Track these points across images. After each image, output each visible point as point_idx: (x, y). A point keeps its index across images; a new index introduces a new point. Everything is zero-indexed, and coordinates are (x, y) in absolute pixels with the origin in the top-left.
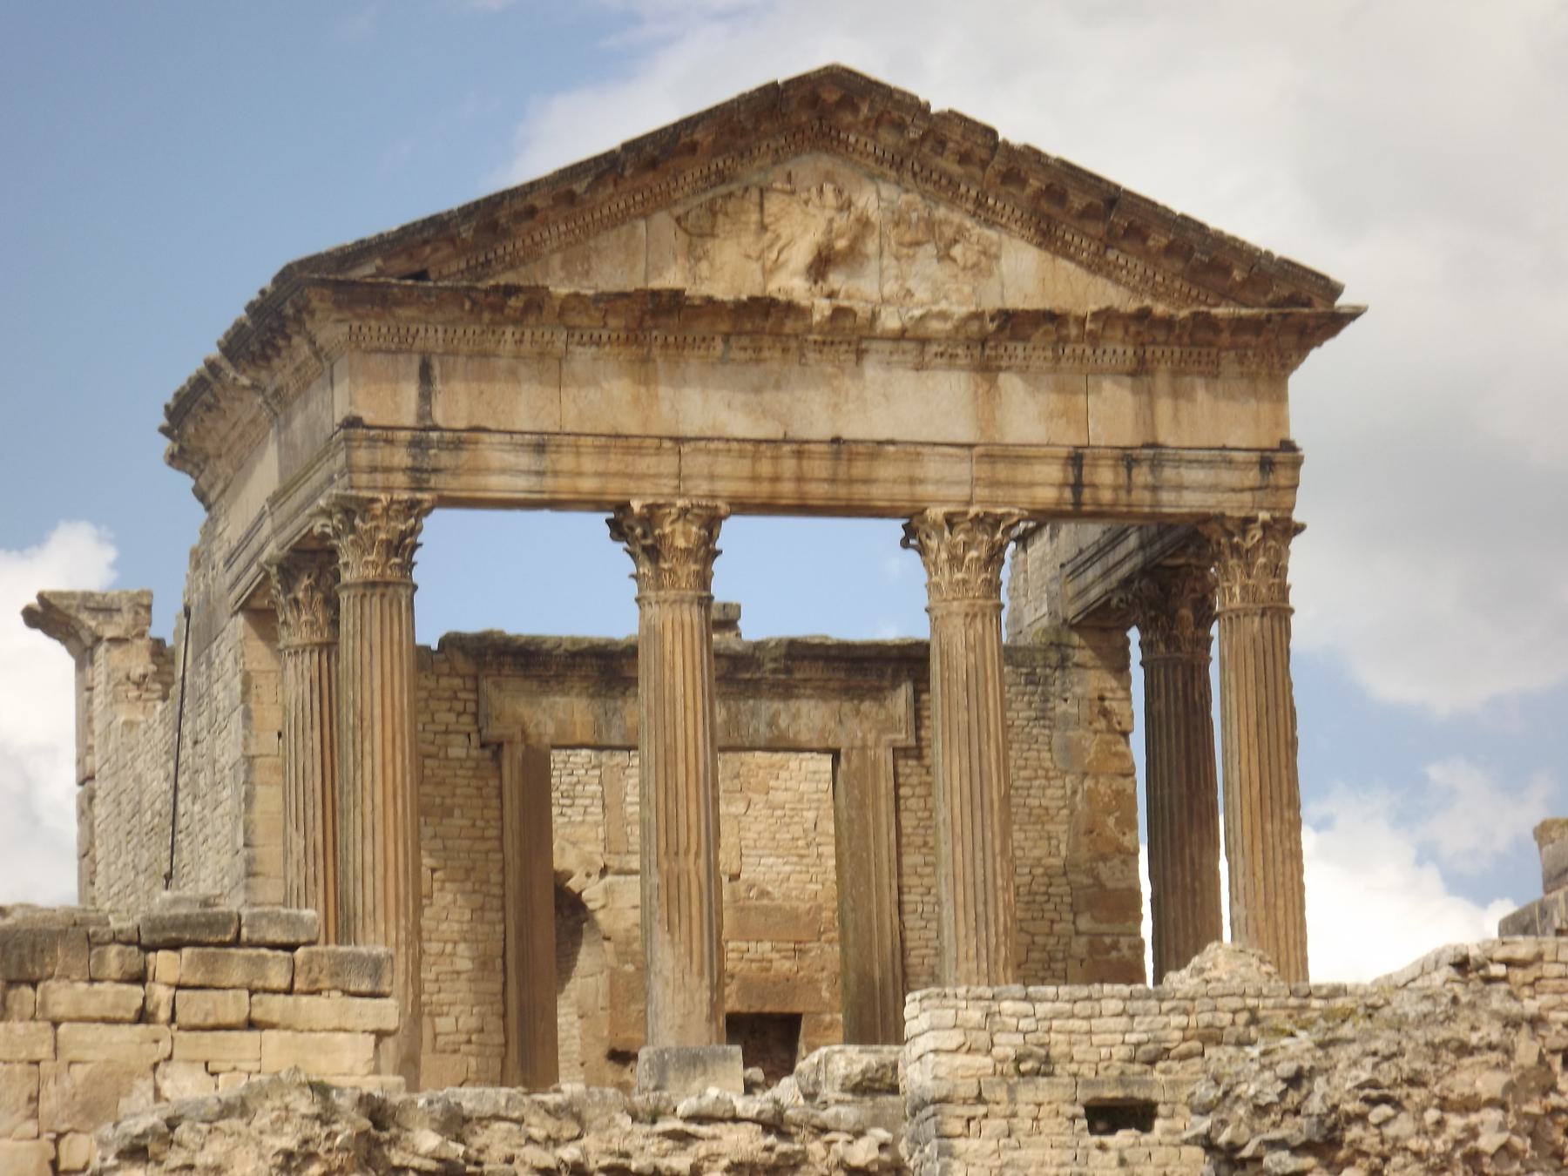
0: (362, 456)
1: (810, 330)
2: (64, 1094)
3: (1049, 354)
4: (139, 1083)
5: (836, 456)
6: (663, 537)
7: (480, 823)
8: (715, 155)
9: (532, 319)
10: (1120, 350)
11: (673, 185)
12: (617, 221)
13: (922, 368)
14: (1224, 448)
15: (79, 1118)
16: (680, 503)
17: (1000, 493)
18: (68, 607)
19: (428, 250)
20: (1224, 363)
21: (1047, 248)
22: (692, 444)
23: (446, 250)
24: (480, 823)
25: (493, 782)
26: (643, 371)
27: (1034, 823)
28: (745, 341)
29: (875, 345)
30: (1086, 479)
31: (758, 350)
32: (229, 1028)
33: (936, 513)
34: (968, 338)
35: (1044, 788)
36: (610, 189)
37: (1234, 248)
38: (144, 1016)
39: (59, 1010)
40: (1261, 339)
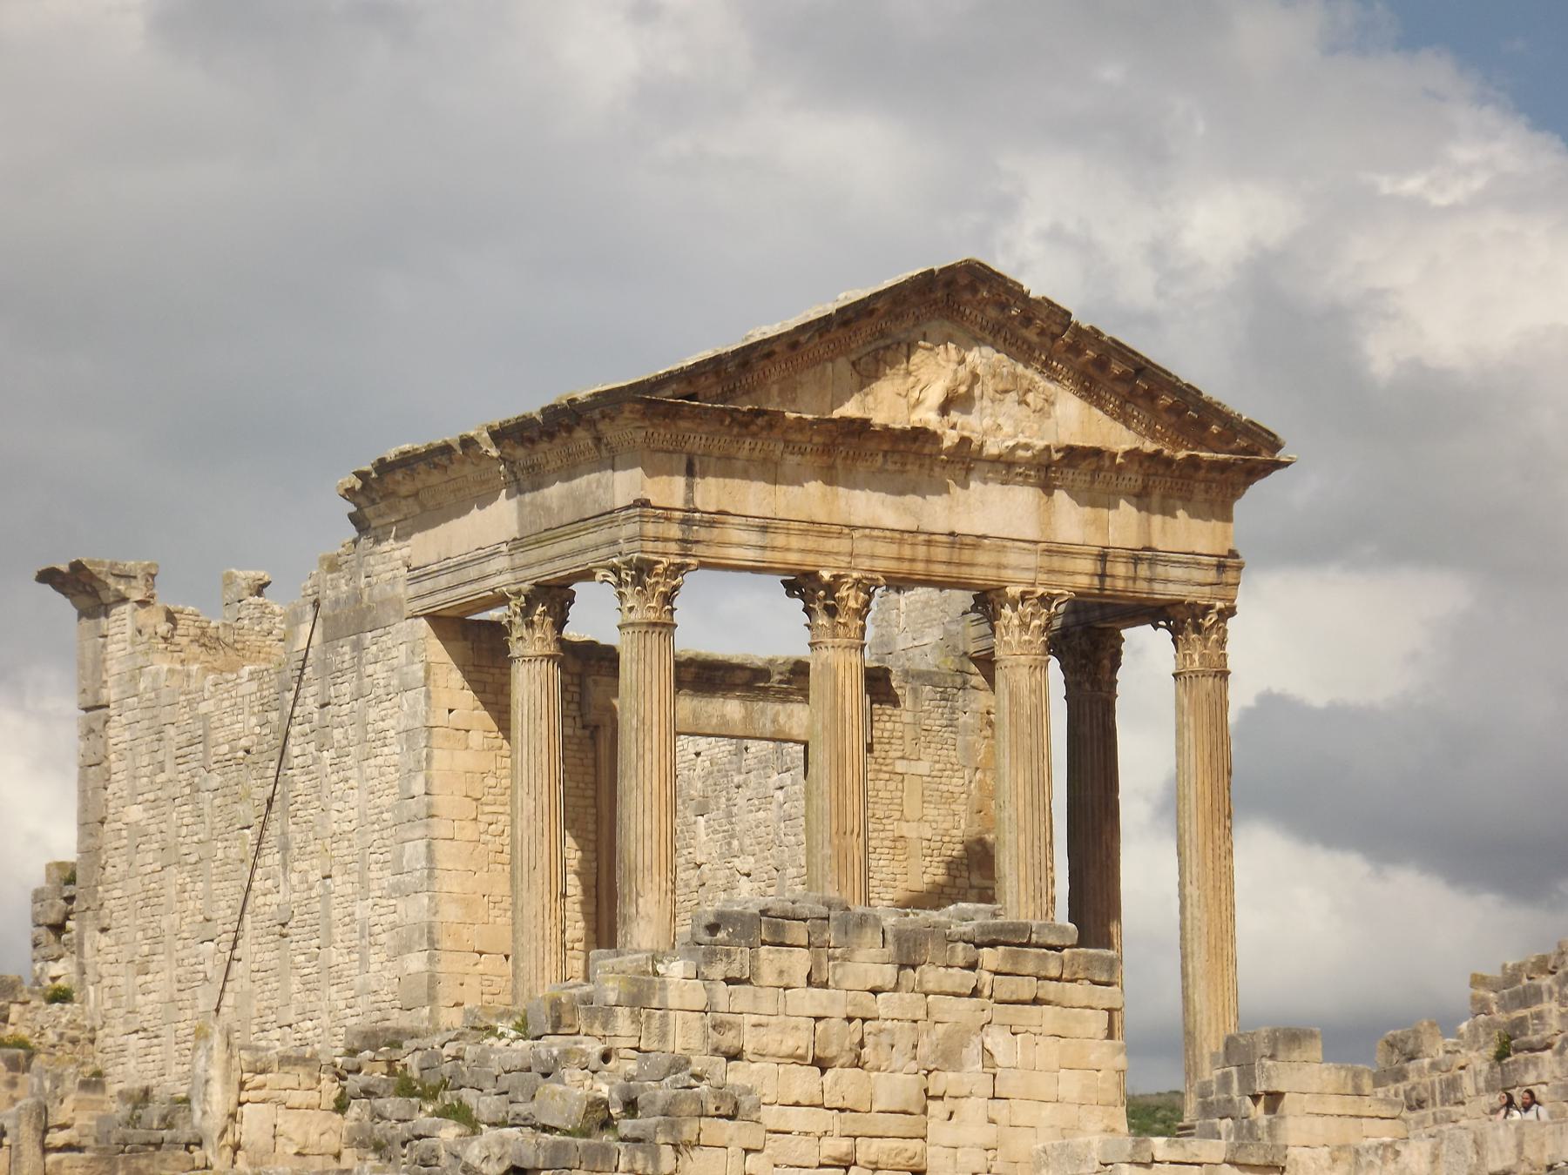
0: (650, 529)
1: (940, 452)
2: (932, 1044)
3: (1088, 478)
4: (973, 1038)
5: (952, 545)
6: (842, 599)
7: (581, 785)
9: (764, 434)
10: (1133, 477)
11: (853, 338)
12: (817, 362)
13: (1006, 484)
14: (1193, 553)
15: (940, 1060)
16: (855, 575)
17: (1054, 578)
18: (100, 573)
19: (703, 379)
20: (1196, 491)
21: (1085, 400)
22: (861, 530)
23: (712, 380)
24: (581, 785)
25: (591, 755)
26: (830, 477)
27: (945, 803)
28: (897, 457)
29: (980, 465)
30: (1108, 571)
31: (904, 464)
32: (1024, 1003)
33: (1013, 591)
34: (1039, 464)
35: (952, 777)
36: (817, 340)
37: (1217, 410)
38: (975, 992)
39: (930, 986)
40: (1224, 476)
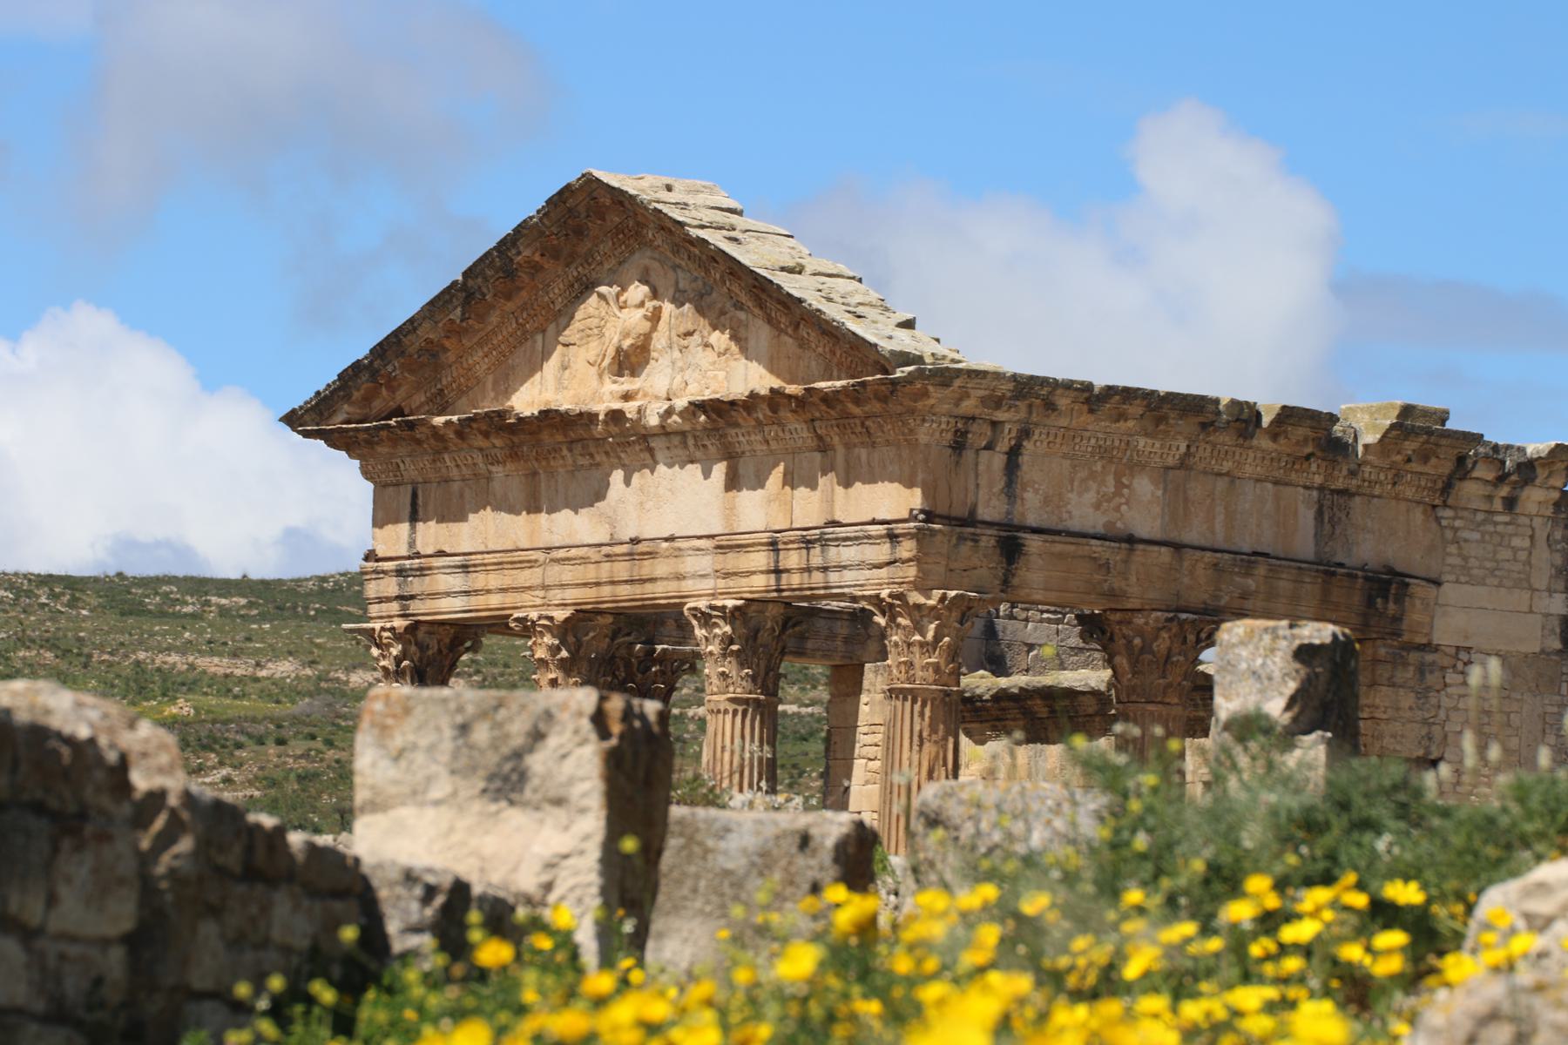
8: (568, 265)
12: (524, 337)
31: (592, 456)
